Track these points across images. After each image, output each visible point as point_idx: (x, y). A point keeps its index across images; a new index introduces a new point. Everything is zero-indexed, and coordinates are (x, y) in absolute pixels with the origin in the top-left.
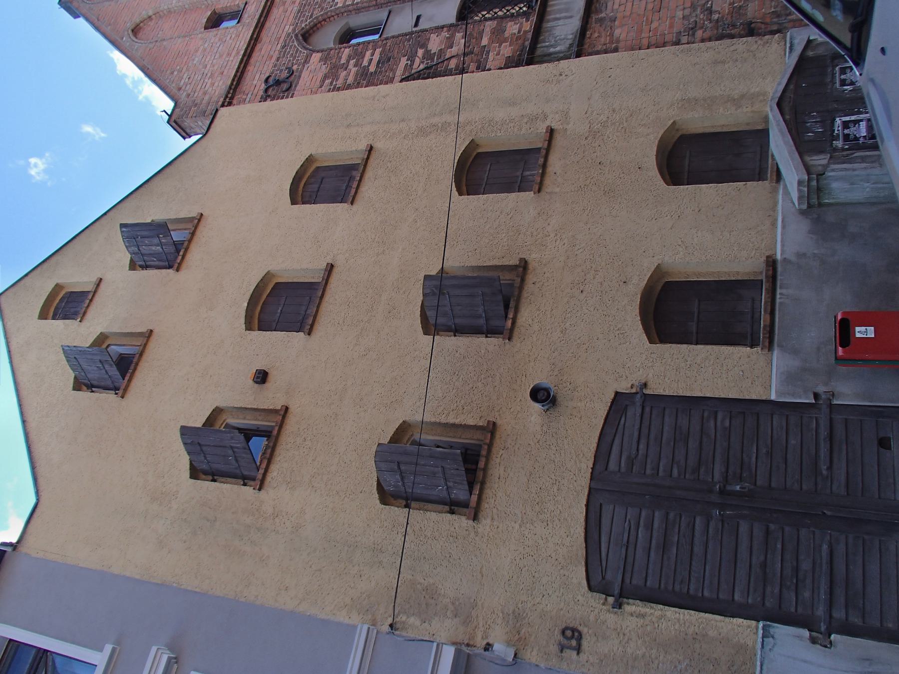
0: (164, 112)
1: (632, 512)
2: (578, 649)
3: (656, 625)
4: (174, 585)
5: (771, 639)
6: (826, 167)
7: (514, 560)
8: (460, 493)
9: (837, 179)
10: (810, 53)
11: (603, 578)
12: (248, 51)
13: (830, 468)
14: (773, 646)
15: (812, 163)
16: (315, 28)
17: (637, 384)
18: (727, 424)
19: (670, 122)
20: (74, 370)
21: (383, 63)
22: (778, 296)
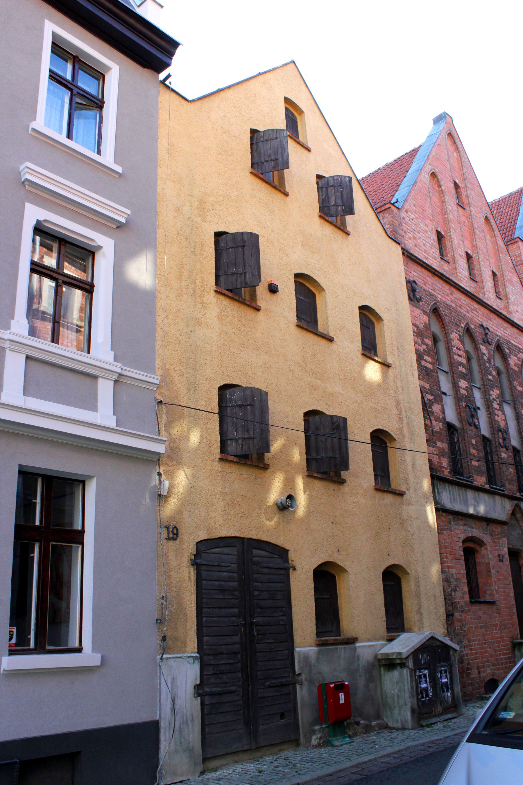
0: (396, 201)
1: (234, 566)
2: (168, 539)
3: (187, 589)
4: (158, 223)
5: (193, 662)
6: (408, 667)
7: (203, 489)
8: (232, 447)
9: (401, 675)
10: (451, 652)
11: (202, 552)
12: (429, 268)
13: (269, 687)
14: (190, 663)
15: (409, 658)
16: (438, 316)
17: (294, 563)
18: (282, 623)
19: (409, 571)
20: (264, 132)
21: (426, 371)
22: (340, 647)
